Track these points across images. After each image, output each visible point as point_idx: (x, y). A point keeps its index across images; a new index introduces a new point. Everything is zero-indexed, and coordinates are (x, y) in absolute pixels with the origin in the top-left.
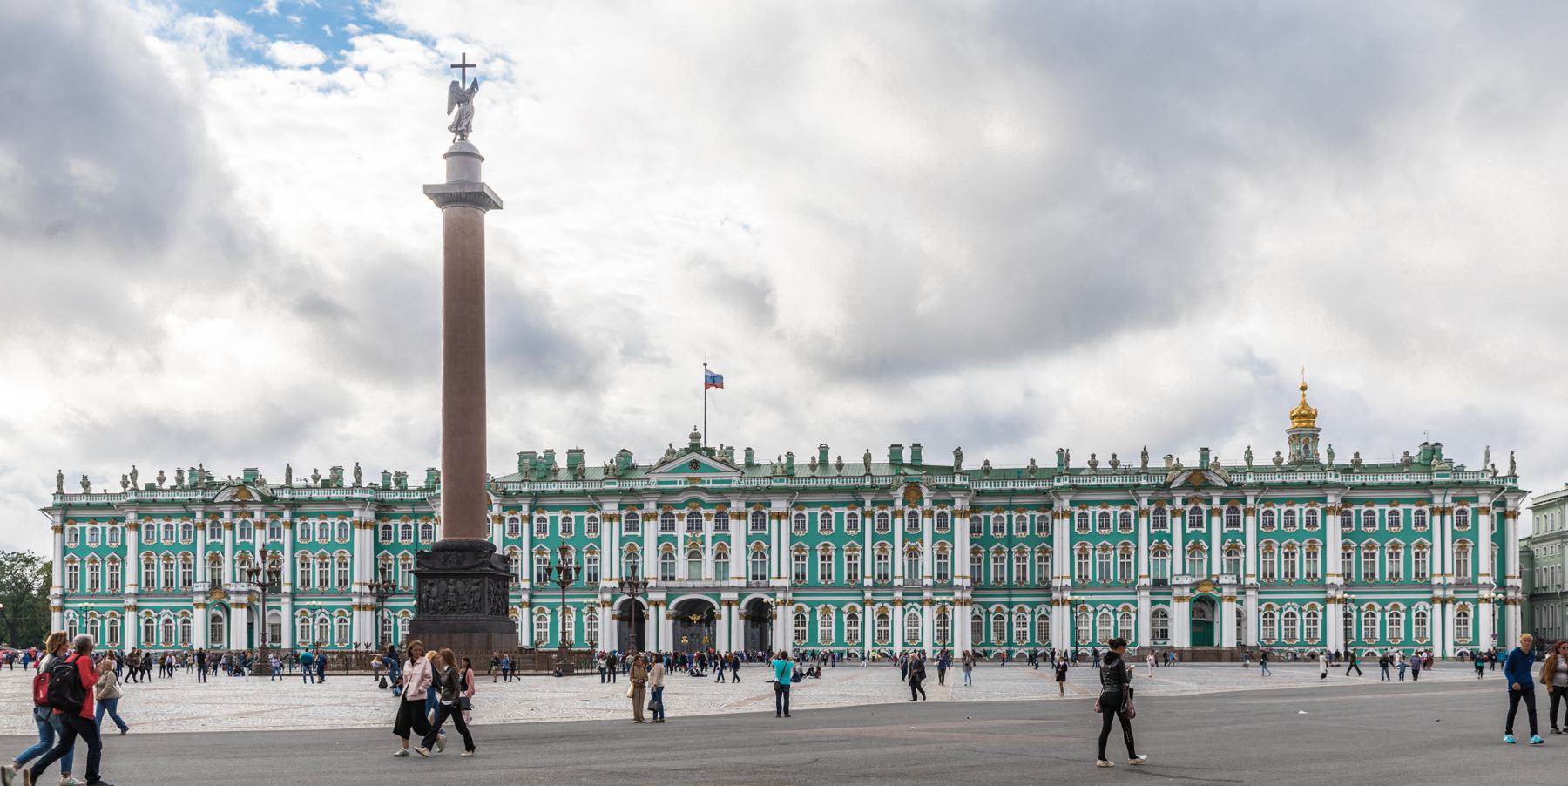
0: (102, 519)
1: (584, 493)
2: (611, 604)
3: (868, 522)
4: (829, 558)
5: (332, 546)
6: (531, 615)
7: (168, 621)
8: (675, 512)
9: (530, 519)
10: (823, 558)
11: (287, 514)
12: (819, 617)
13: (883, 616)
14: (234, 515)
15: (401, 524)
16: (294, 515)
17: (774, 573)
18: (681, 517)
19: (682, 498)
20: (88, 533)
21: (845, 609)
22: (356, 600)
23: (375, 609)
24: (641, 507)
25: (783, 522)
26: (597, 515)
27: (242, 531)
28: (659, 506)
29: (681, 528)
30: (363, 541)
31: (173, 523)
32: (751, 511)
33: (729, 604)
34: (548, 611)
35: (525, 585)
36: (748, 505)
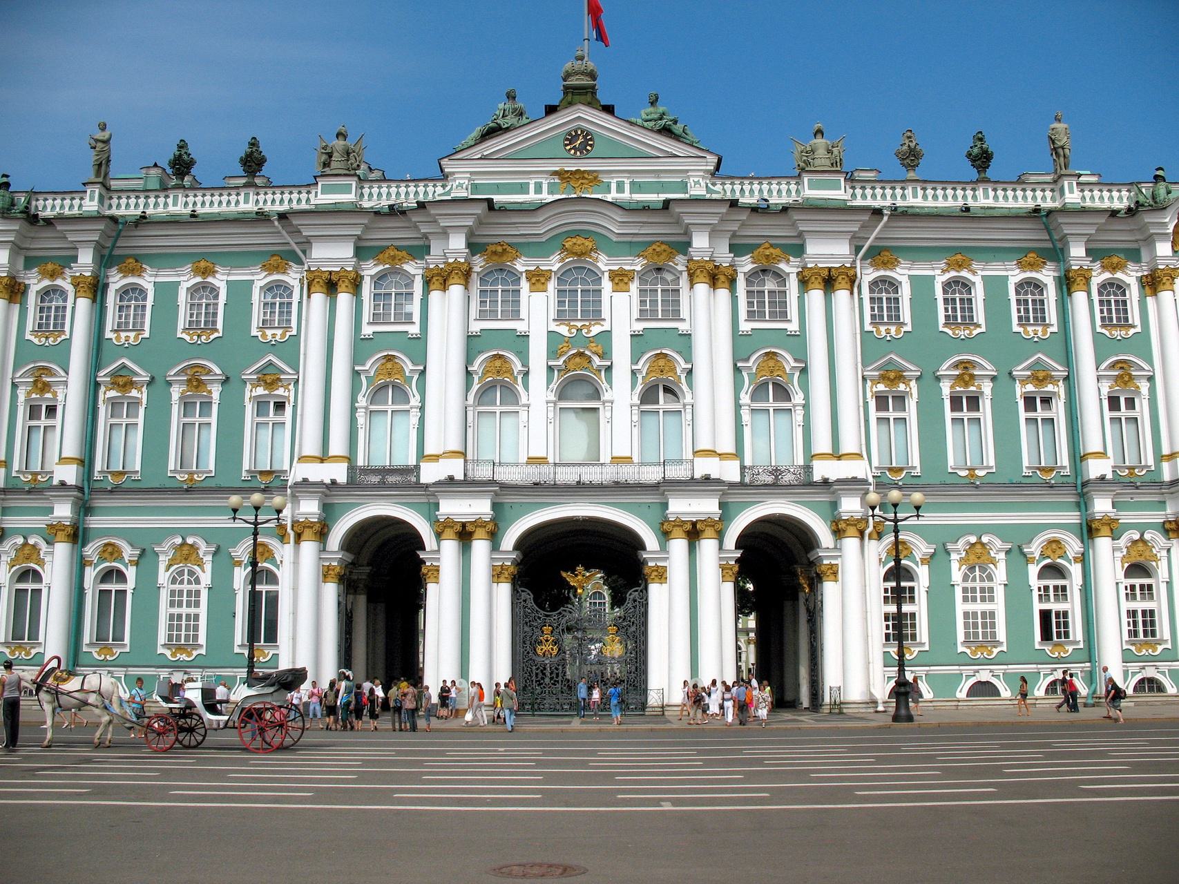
2: (322, 534)
3: (1080, 298)
4: (974, 402)
6: (81, 564)
8: (521, 265)
9: (96, 289)
10: (956, 403)
12: (957, 575)
13: (1137, 569)
17: (822, 444)
18: (538, 279)
19: (543, 227)
21: (1035, 549)
24: (420, 251)
25: (841, 296)
26: (293, 277)
28: (473, 247)
29: (537, 312)
32: (746, 265)
33: (694, 533)
34: (128, 552)
35: (69, 474)
36: (736, 249)
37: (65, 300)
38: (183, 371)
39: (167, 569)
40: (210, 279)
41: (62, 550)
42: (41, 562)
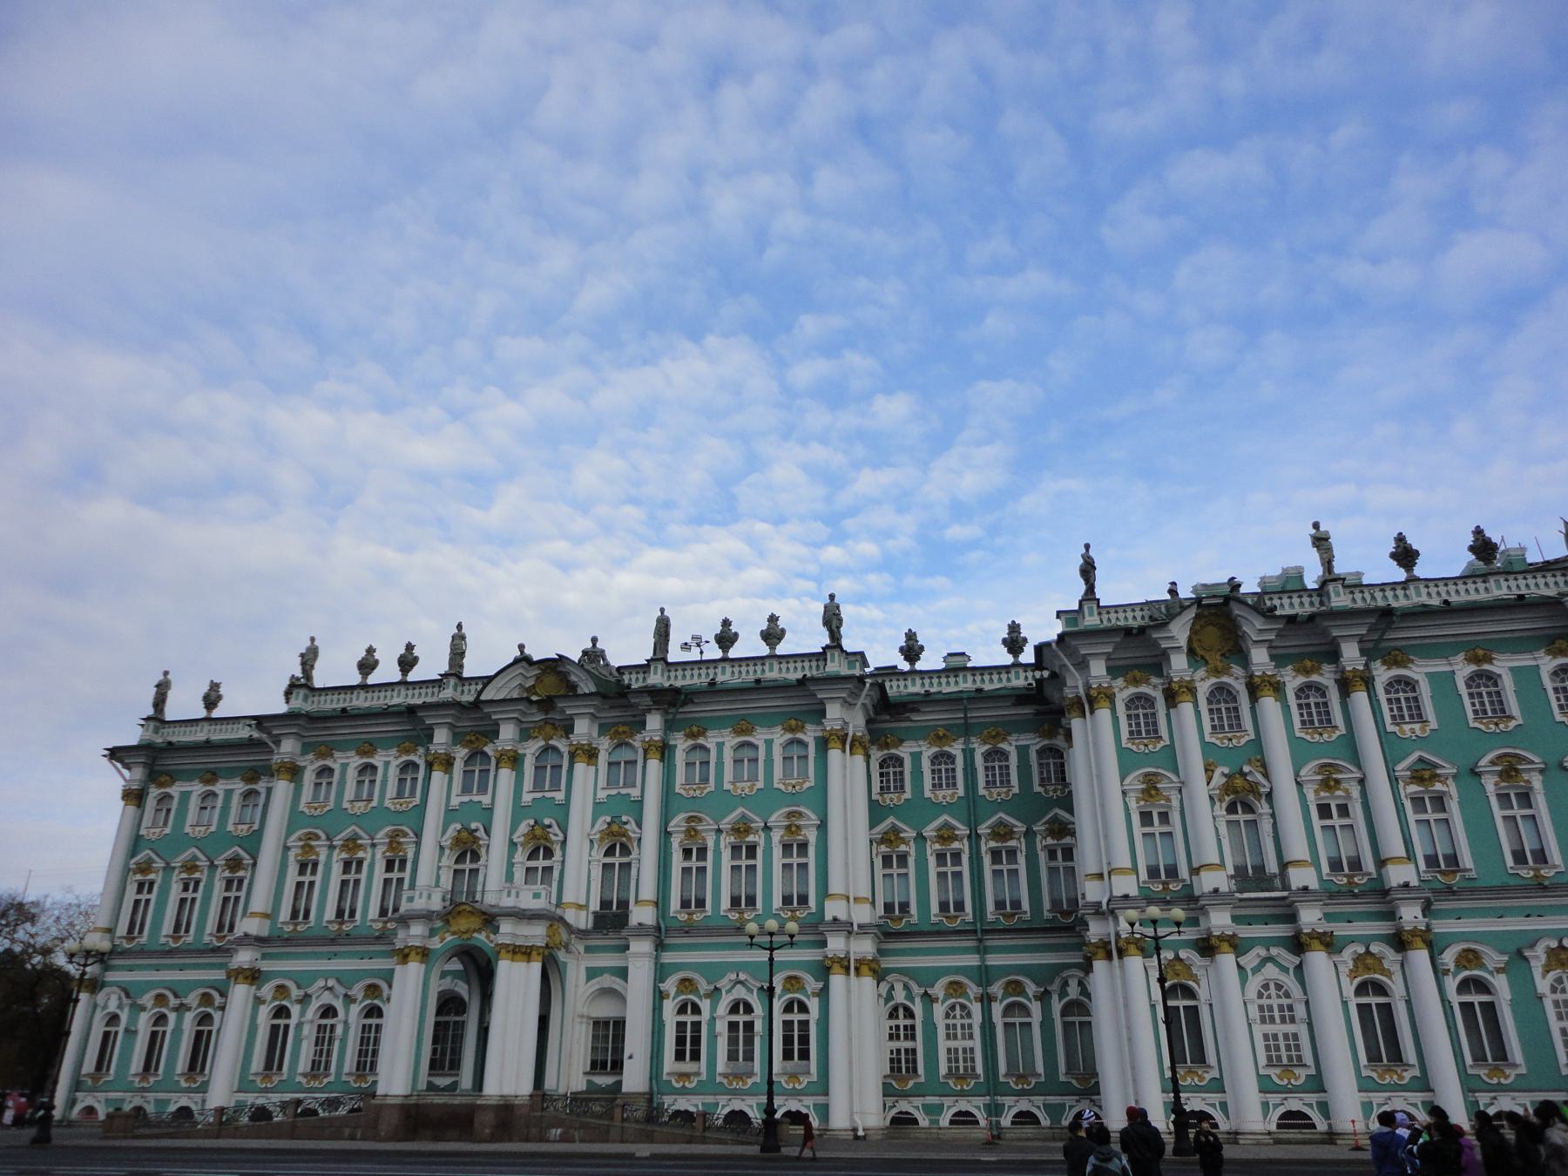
0: (230, 773)
1: (1521, 603)
5: (770, 797)
6: (1439, 973)
7: (329, 1011)
11: (654, 722)
14: (525, 735)
15: (927, 752)
16: (670, 726)
20: (194, 802)
22: (836, 944)
23: (880, 975)
27: (539, 769)
30: (849, 777)
31: (378, 760)
34: (1493, 958)
37: (1323, 695)
38: (1493, 763)
39: (1544, 976)
40: (1486, 667)
41: (1420, 958)
42: (1389, 974)
